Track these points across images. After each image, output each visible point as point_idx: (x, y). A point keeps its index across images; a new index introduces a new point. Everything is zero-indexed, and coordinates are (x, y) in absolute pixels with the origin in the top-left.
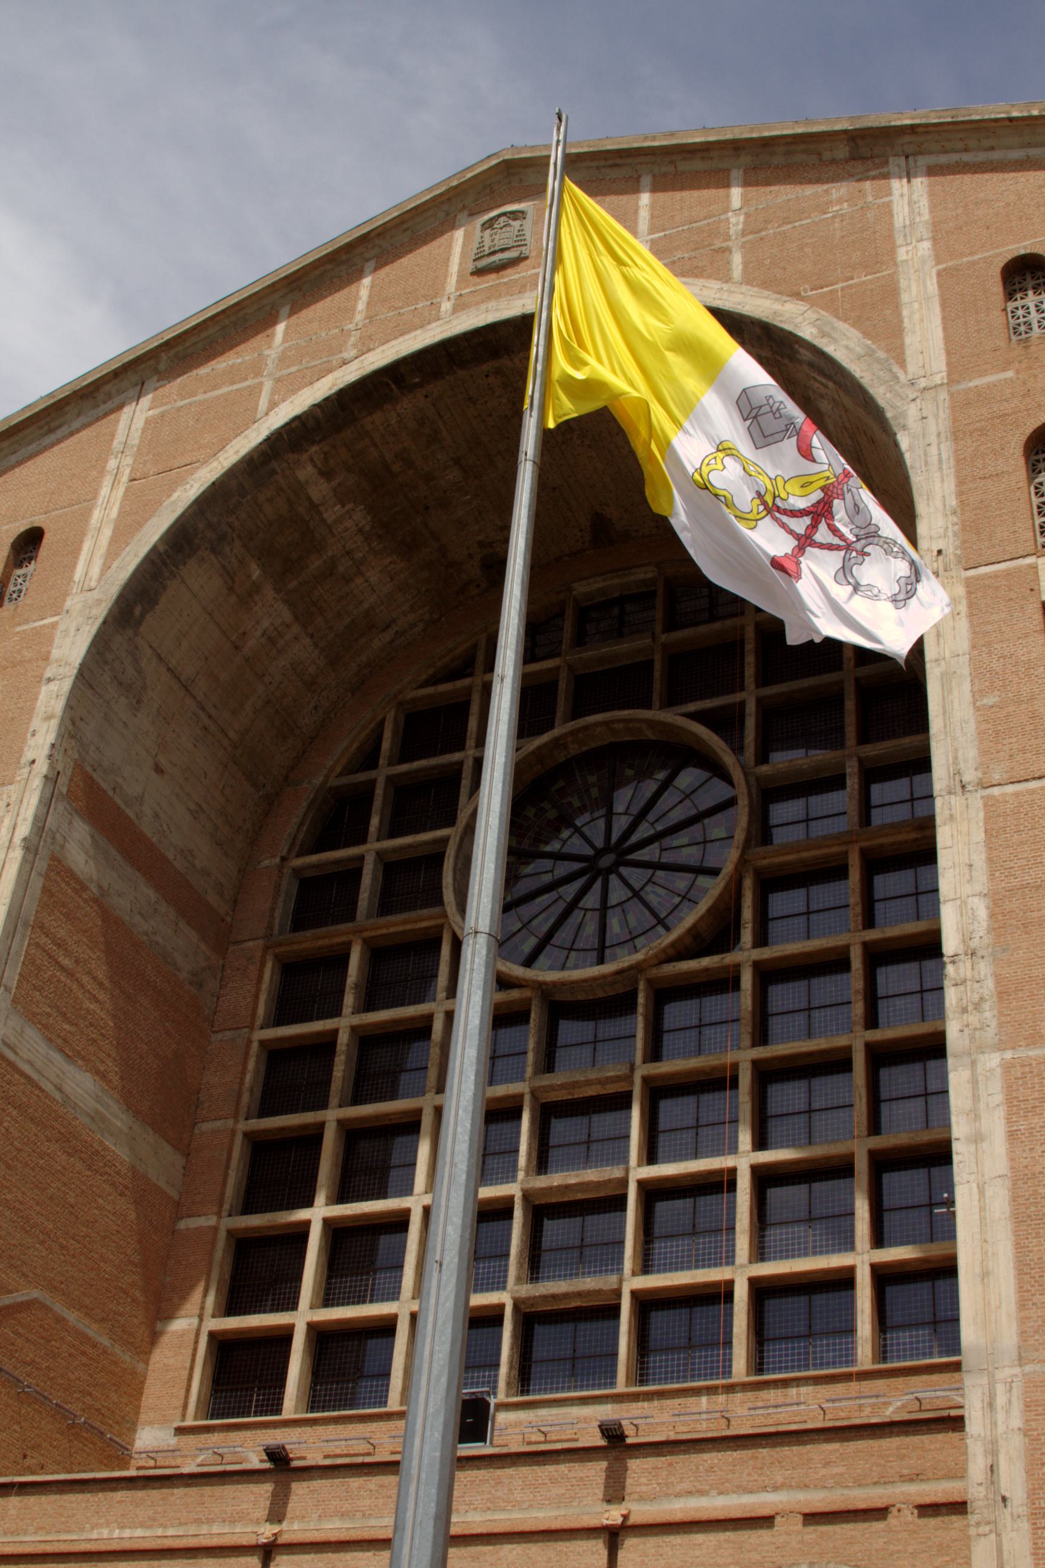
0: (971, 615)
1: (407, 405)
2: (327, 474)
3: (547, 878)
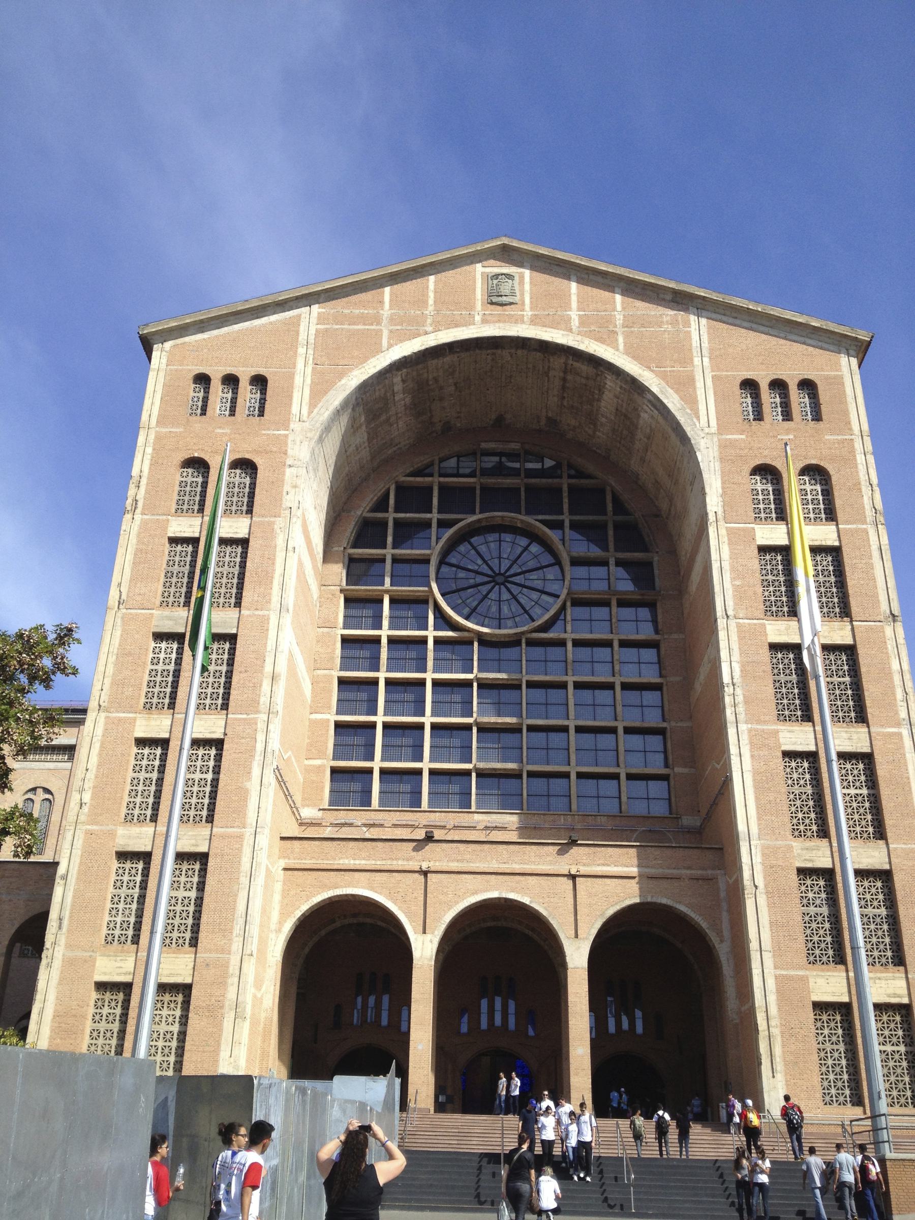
0: (729, 544)
1: (448, 359)
2: (403, 381)
3: (472, 581)
